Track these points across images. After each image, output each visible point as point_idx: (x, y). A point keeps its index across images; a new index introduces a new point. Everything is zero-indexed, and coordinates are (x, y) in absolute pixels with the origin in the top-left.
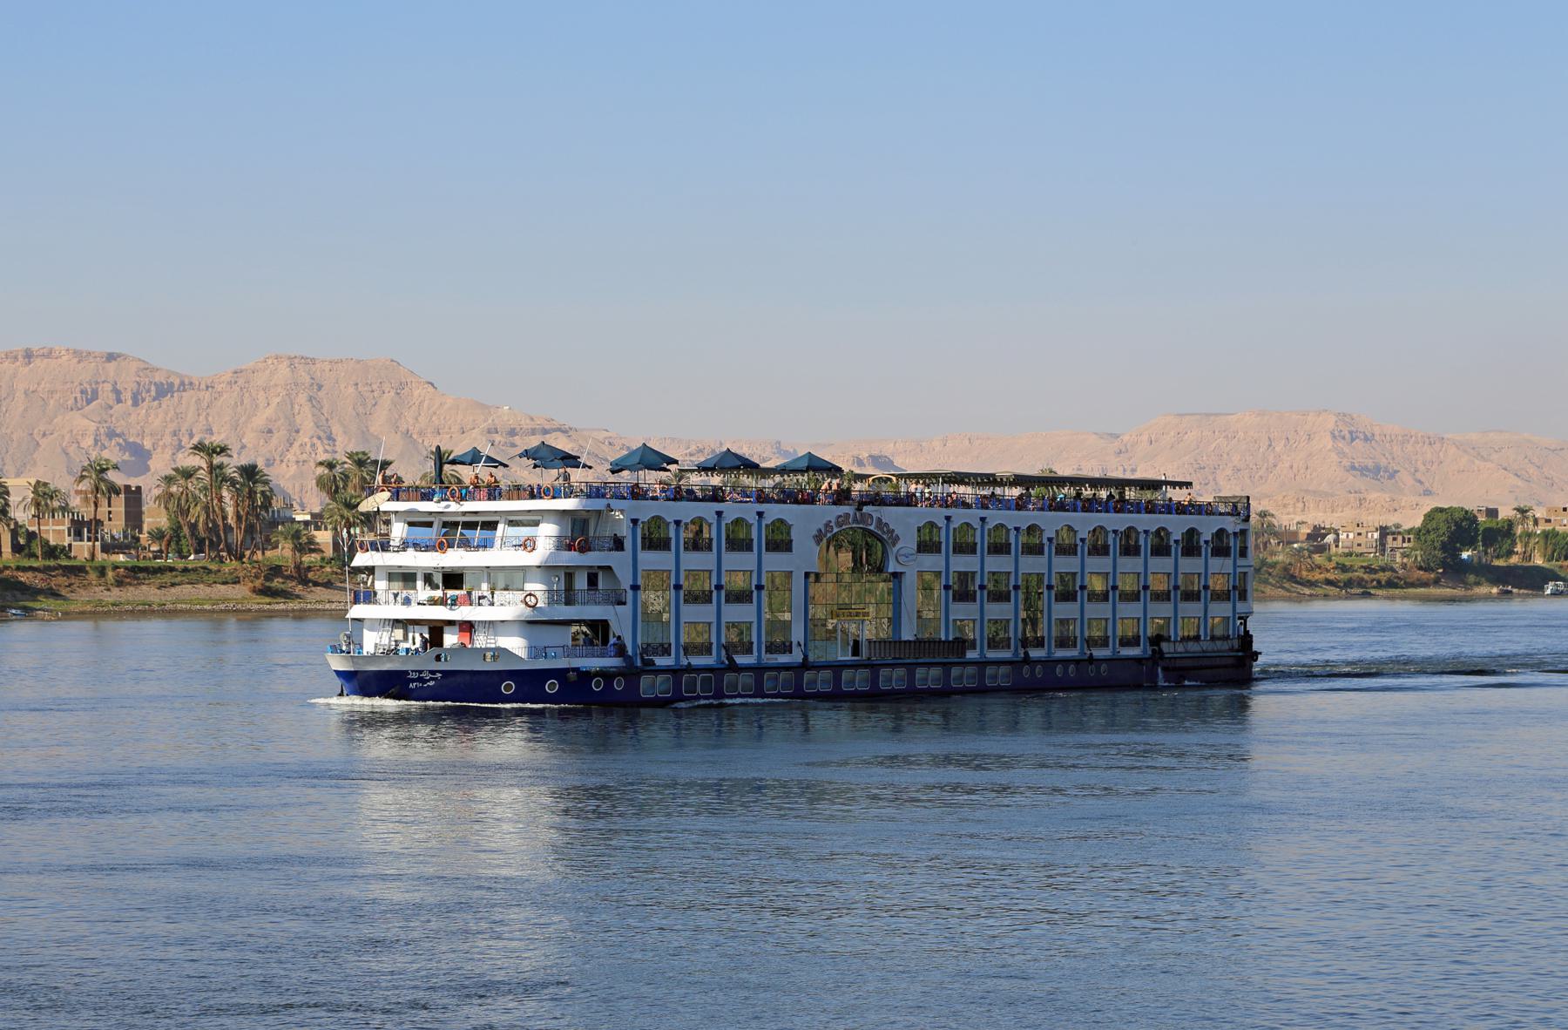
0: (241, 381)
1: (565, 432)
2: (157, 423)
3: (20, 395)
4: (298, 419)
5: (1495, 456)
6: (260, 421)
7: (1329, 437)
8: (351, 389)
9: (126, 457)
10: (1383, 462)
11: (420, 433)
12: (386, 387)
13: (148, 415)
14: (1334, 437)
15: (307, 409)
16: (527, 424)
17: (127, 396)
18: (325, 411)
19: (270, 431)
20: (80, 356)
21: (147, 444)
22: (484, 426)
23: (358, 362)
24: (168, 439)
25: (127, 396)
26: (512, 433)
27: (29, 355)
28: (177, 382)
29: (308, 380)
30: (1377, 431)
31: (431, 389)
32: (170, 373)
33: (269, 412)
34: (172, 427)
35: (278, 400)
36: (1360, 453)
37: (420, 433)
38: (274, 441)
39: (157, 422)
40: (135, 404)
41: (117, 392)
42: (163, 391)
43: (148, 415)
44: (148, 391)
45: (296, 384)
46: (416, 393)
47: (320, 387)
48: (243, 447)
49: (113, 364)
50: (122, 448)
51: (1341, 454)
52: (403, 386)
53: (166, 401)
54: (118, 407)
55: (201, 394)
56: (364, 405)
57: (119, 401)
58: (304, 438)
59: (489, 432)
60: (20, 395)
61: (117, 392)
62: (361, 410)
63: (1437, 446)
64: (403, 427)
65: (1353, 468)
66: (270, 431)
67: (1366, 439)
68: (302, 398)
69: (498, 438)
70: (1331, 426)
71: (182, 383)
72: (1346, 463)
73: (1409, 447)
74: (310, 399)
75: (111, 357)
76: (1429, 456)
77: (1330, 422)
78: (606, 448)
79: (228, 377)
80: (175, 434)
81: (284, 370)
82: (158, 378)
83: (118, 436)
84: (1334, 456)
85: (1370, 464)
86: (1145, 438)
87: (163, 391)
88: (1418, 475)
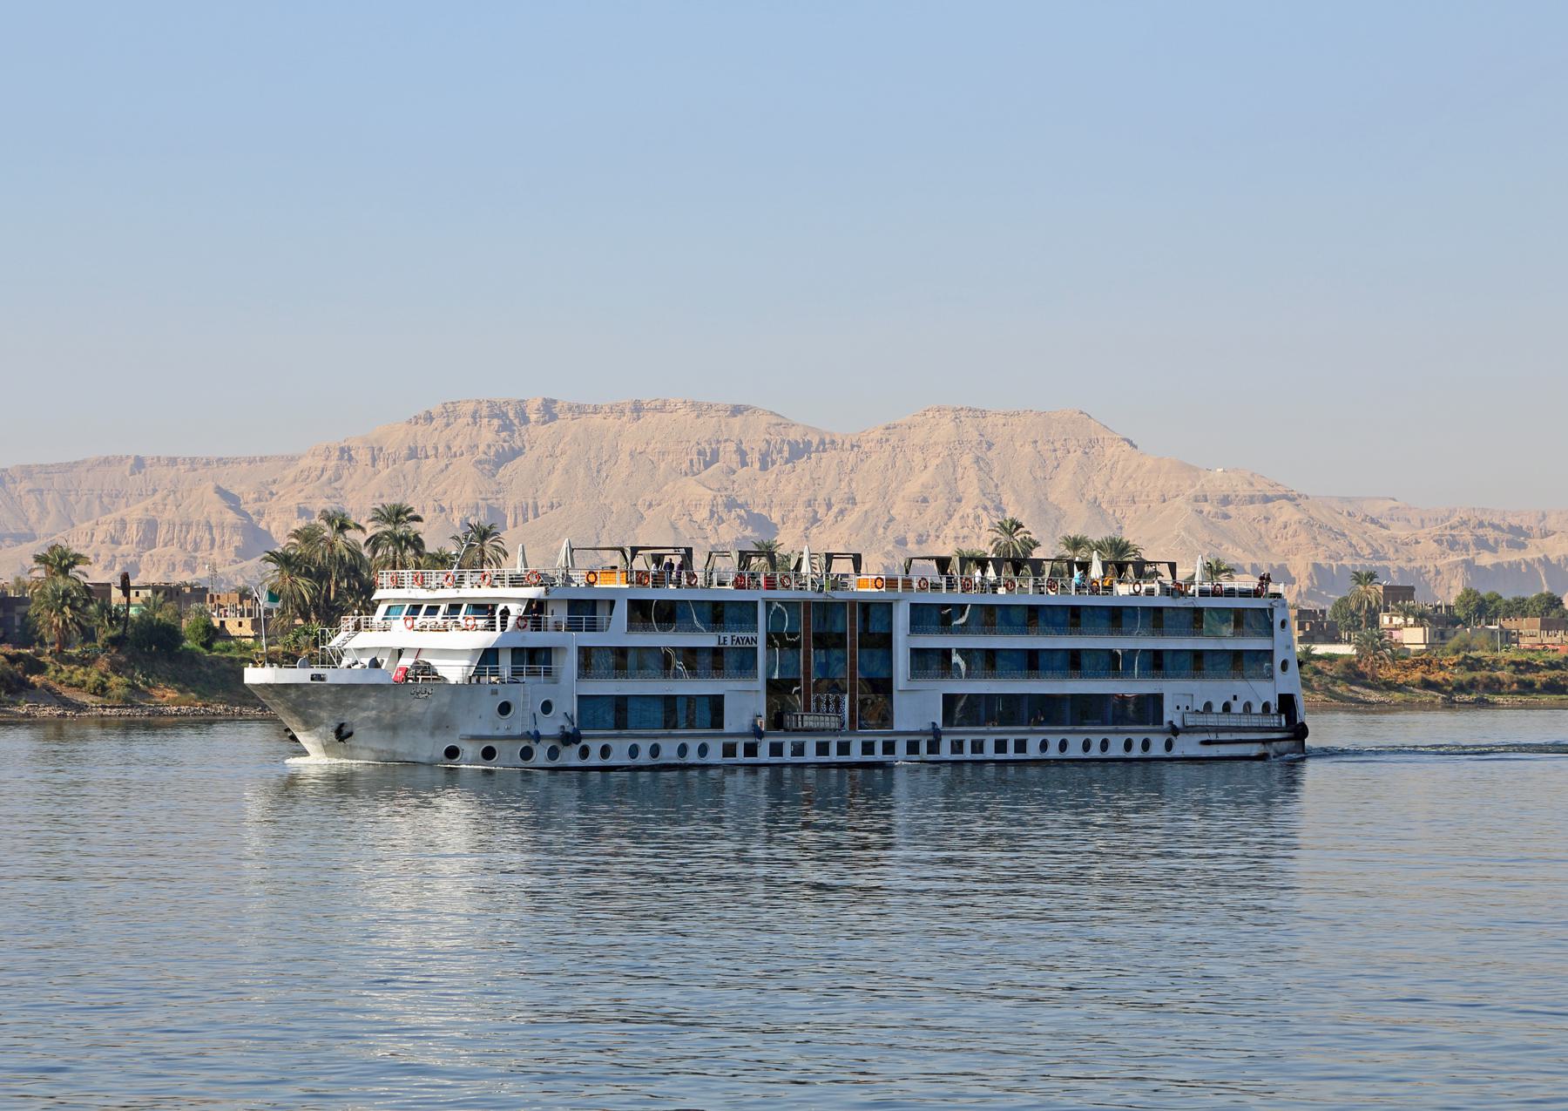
0: (894, 440)
3: (624, 457)
6: (913, 487)
8: (1028, 448)
9: (748, 532)
11: (1111, 502)
12: (1072, 444)
13: (778, 481)
15: (972, 473)
16: (1244, 490)
17: (754, 457)
18: (994, 475)
19: (925, 500)
20: (699, 409)
21: (776, 517)
22: (1191, 492)
24: (800, 510)
25: (754, 457)
26: (1226, 501)
27: (638, 408)
29: (974, 436)
31: (1127, 447)
33: (925, 477)
35: (938, 461)
37: (1111, 502)
38: (930, 513)
39: (789, 490)
40: (764, 467)
41: (742, 454)
42: (798, 451)
43: (778, 481)
44: (780, 452)
46: (1109, 452)
47: (990, 446)
48: (891, 520)
50: (744, 522)
53: (801, 464)
54: (742, 472)
56: (1043, 466)
57: (744, 464)
58: (966, 509)
60: (624, 457)
61: (742, 454)
62: (1039, 474)
64: (1090, 496)
66: (925, 500)
68: (967, 460)
69: (1207, 508)
71: (822, 442)
74: (977, 460)
75: (737, 410)
78: (1343, 520)
79: (877, 435)
80: (809, 504)
81: (947, 426)
82: (794, 435)
83: (740, 506)
87: (798, 451)
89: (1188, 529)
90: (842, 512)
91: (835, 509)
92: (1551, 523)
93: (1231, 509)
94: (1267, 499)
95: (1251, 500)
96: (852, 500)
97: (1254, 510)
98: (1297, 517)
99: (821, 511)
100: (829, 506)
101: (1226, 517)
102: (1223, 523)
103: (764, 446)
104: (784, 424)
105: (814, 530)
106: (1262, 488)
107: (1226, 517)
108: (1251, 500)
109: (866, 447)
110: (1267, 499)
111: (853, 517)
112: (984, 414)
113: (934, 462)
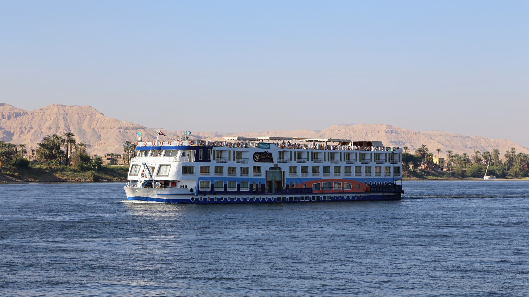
0: (42, 112)
1: (144, 129)
2: (15, 125)
4: (59, 124)
5: (436, 138)
6: (47, 125)
7: (384, 132)
8: (77, 115)
9: (5, 136)
10: (401, 140)
12: (88, 114)
13: (12, 123)
14: (386, 132)
15: (62, 121)
16: (131, 126)
17: (6, 117)
19: (50, 128)
21: (12, 131)
22: (117, 127)
23: (79, 106)
24: (18, 130)
25: (6, 117)
26: (127, 129)
28: (22, 112)
29: (63, 112)
30: (399, 130)
31: (102, 115)
32: (20, 110)
33: (50, 122)
34: (20, 126)
36: (394, 137)
39: (15, 125)
40: (9, 119)
42: (18, 115)
43: (12, 123)
44: (13, 115)
45: (59, 113)
47: (67, 114)
48: (42, 133)
49: (2, 106)
50: (4, 133)
51: (388, 137)
52: (93, 114)
53: (18, 118)
54: (3, 120)
55: (29, 116)
56: (80, 120)
57: (3, 118)
59: (119, 128)
62: (79, 122)
63: (418, 135)
64: (92, 127)
65: (392, 141)
66: (50, 128)
67: (396, 133)
68: (61, 118)
69: (122, 130)
70: (385, 128)
71: (24, 113)
72: (390, 140)
73: (409, 135)
74: (64, 118)
76: (415, 138)
77: (385, 127)
80: (20, 128)
81: (56, 109)
82: (16, 111)
83: (3, 129)
84: (386, 138)
85: (397, 140)
86: (328, 132)
87: (18, 115)
88: (412, 144)
89: (117, 136)
90: (29, 131)
91: (27, 130)
92: (206, 135)
93: (128, 131)
94: (137, 129)
95: (133, 129)
96: (32, 128)
97: (133, 131)
98: (145, 133)
99: (24, 130)
100: (26, 129)
101: (127, 133)
102: (126, 134)
103: (9, 114)
104: (13, 108)
105: (22, 135)
106: (135, 126)
107: (127, 133)
108: (133, 129)
109: (35, 114)
110: (137, 129)
111: (32, 132)
112: (65, 106)
113: (52, 118)
